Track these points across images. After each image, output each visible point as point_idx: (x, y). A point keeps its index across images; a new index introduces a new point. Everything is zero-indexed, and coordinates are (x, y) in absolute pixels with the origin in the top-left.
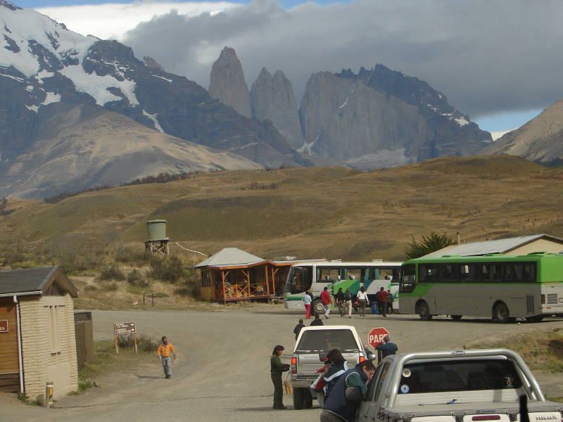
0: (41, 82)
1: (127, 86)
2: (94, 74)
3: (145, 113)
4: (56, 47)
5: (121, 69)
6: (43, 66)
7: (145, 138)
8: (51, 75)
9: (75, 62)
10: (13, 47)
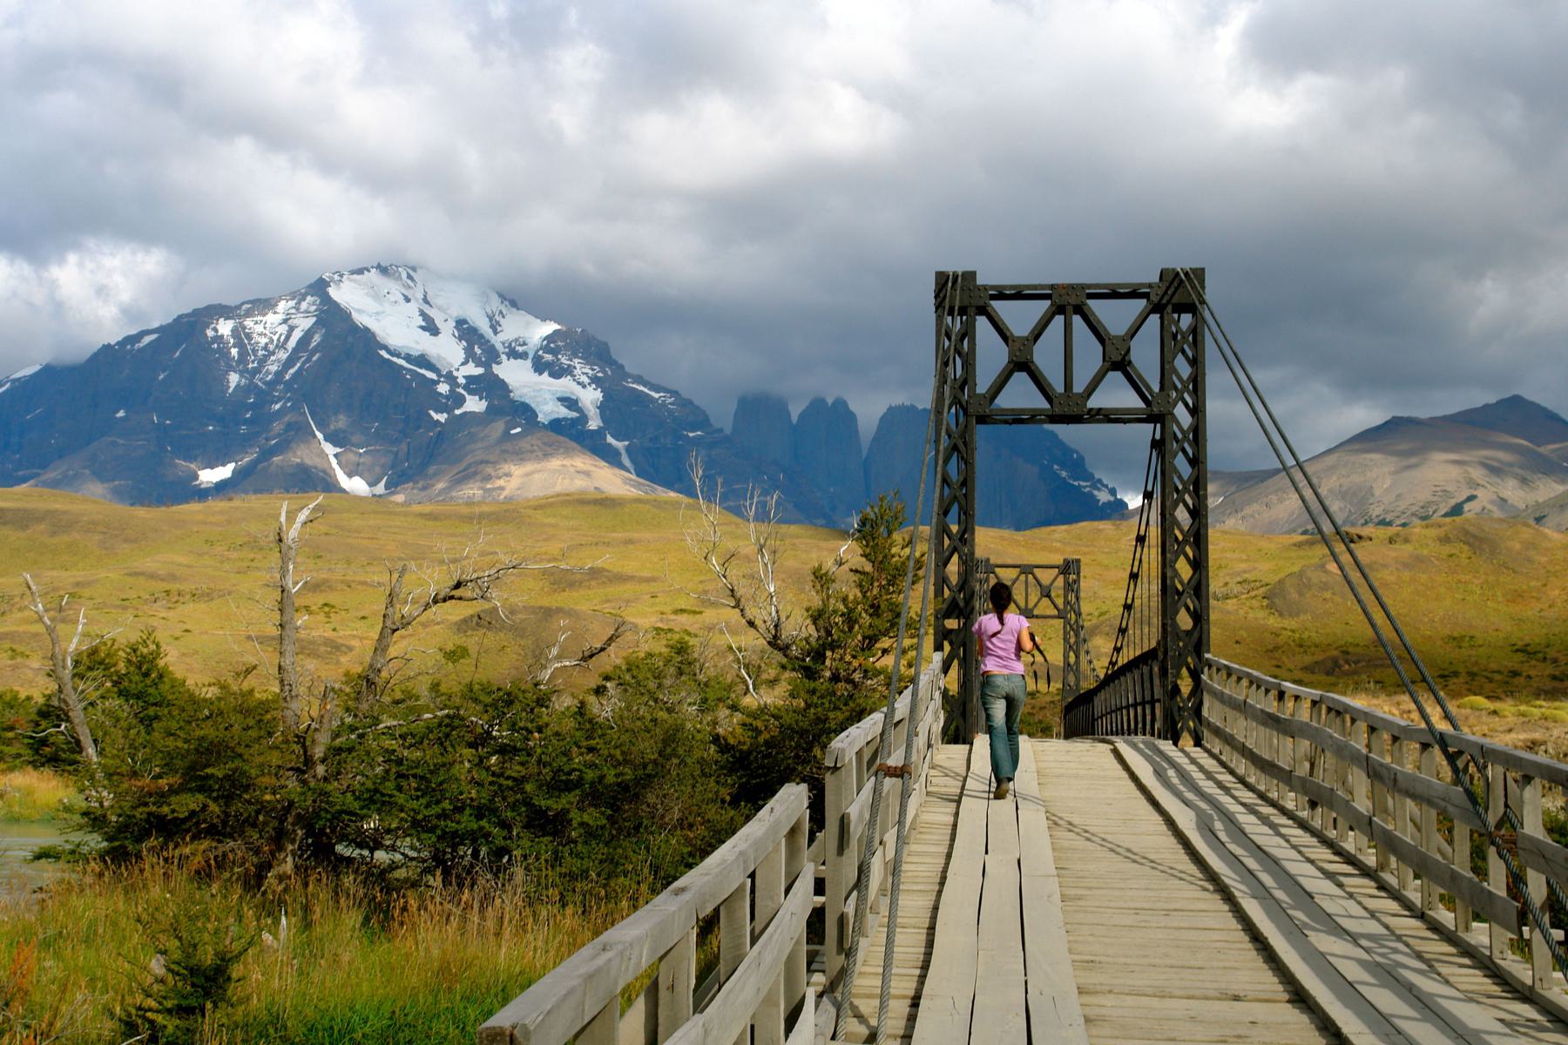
0: (462, 381)
1: (590, 397)
2: (546, 374)
3: (610, 439)
4: (496, 333)
5: (582, 369)
6: (470, 355)
7: (587, 474)
8: (480, 371)
9: (524, 356)
10: (431, 328)
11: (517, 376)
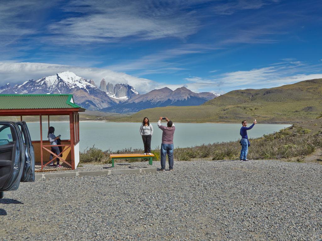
1: (85, 86)
11: (77, 83)
